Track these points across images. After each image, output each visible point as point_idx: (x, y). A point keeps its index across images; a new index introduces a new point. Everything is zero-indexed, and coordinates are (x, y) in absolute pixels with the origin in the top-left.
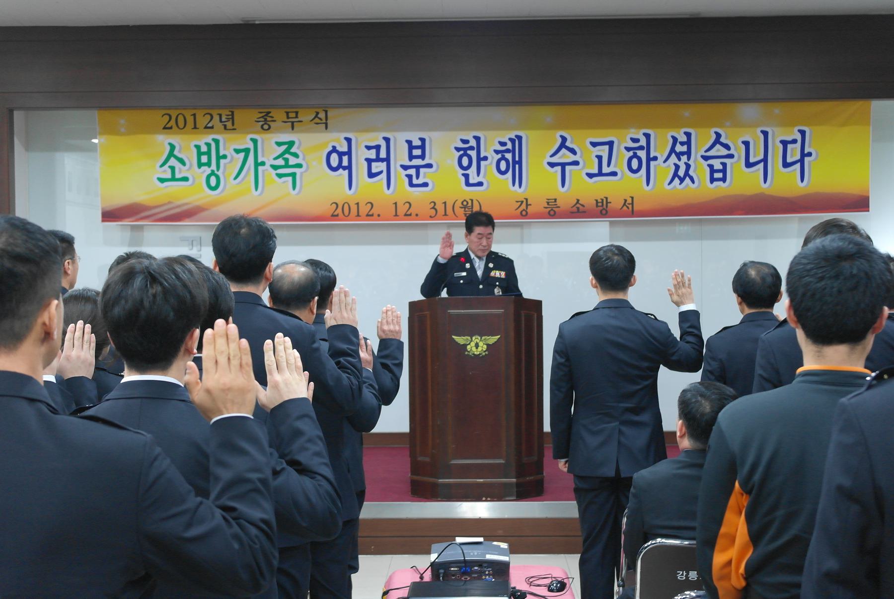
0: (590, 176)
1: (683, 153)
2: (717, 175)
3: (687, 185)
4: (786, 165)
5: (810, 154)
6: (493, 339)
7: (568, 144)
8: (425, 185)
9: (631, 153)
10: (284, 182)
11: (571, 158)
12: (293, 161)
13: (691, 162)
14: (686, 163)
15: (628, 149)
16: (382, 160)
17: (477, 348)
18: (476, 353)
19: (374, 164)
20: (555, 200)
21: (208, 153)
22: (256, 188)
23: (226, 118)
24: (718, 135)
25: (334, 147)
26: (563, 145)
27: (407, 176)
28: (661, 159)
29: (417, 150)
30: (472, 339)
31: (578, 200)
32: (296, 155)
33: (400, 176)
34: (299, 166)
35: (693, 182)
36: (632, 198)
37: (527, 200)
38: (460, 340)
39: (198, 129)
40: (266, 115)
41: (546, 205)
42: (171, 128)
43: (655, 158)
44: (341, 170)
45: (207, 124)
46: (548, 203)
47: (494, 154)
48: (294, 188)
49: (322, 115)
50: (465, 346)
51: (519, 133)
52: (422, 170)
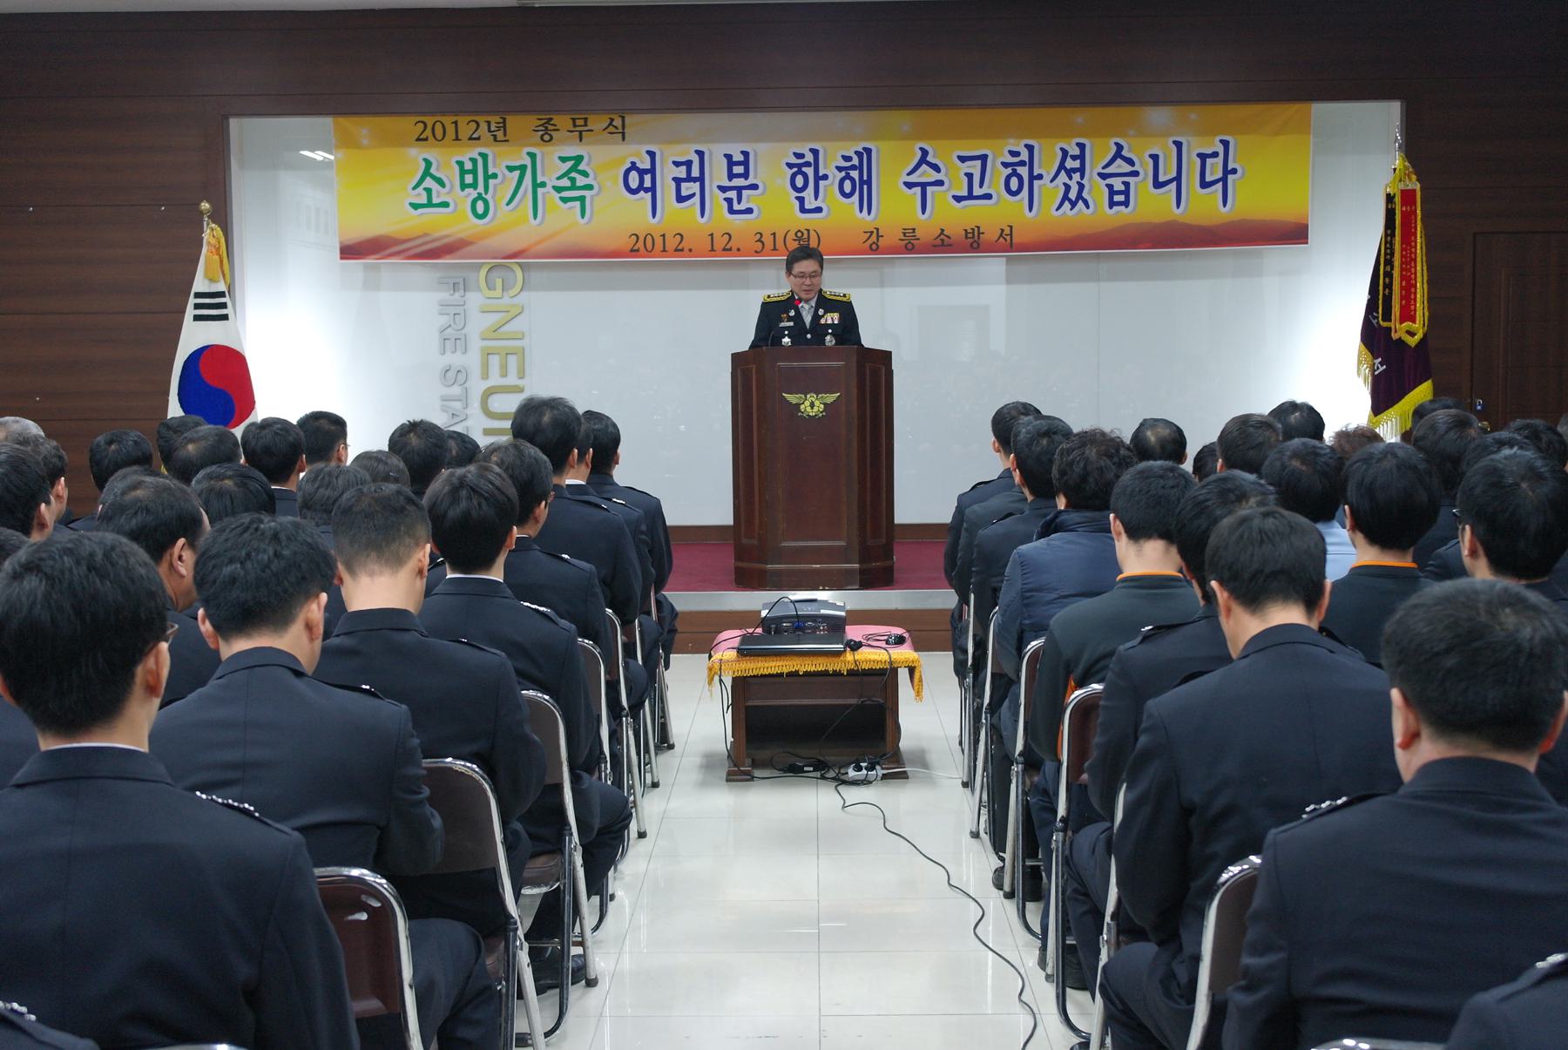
0: (958, 199)
1: (1074, 170)
2: (1118, 198)
3: (1080, 210)
4: (1205, 184)
5: (1234, 171)
6: (831, 398)
8: (749, 211)
9: (1009, 170)
10: (571, 208)
11: (932, 176)
12: (581, 181)
14: (1078, 183)
15: (1005, 165)
16: (694, 180)
17: (812, 408)
18: (811, 414)
19: (684, 185)
20: (914, 229)
21: (474, 172)
22: (535, 217)
24: (1120, 147)
25: (633, 164)
26: (923, 160)
27: (725, 199)
28: (1047, 178)
29: (739, 166)
30: (806, 397)
31: (943, 230)
32: (585, 174)
33: (716, 200)
34: (590, 187)
35: (1088, 207)
36: (1011, 227)
37: (877, 229)
38: (792, 398)
42: (426, 139)
43: (1040, 177)
46: (904, 234)
48: (583, 215)
49: (618, 122)
50: (798, 405)
51: (867, 145)
52: (745, 193)
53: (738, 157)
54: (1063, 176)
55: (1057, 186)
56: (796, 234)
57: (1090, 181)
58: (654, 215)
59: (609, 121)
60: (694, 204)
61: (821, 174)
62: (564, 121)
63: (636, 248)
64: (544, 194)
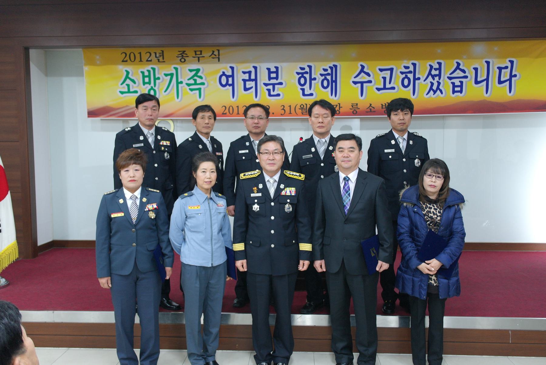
0: (379, 89)
1: (436, 75)
2: (456, 89)
3: (438, 95)
4: (500, 82)
5: (515, 76)
7: (365, 70)
8: (278, 95)
9: (404, 76)
10: (194, 94)
11: (367, 78)
12: (199, 81)
14: (438, 82)
15: (402, 73)
16: (252, 80)
19: (247, 83)
21: (149, 76)
22: (178, 98)
23: (159, 55)
24: (458, 64)
25: (224, 72)
26: (362, 71)
27: (267, 89)
28: (422, 79)
31: (371, 105)
32: (201, 77)
33: (263, 90)
34: (203, 84)
35: (442, 93)
37: (339, 104)
39: (142, 61)
40: (183, 53)
41: (352, 108)
42: (126, 61)
43: (419, 79)
44: (228, 86)
46: (352, 106)
48: (200, 97)
49: (216, 53)
52: (276, 86)
54: (430, 78)
55: (427, 83)
57: (443, 80)
59: (212, 52)
60: (252, 92)
61: (312, 78)
62: (190, 52)
63: (225, 112)
64: (182, 87)
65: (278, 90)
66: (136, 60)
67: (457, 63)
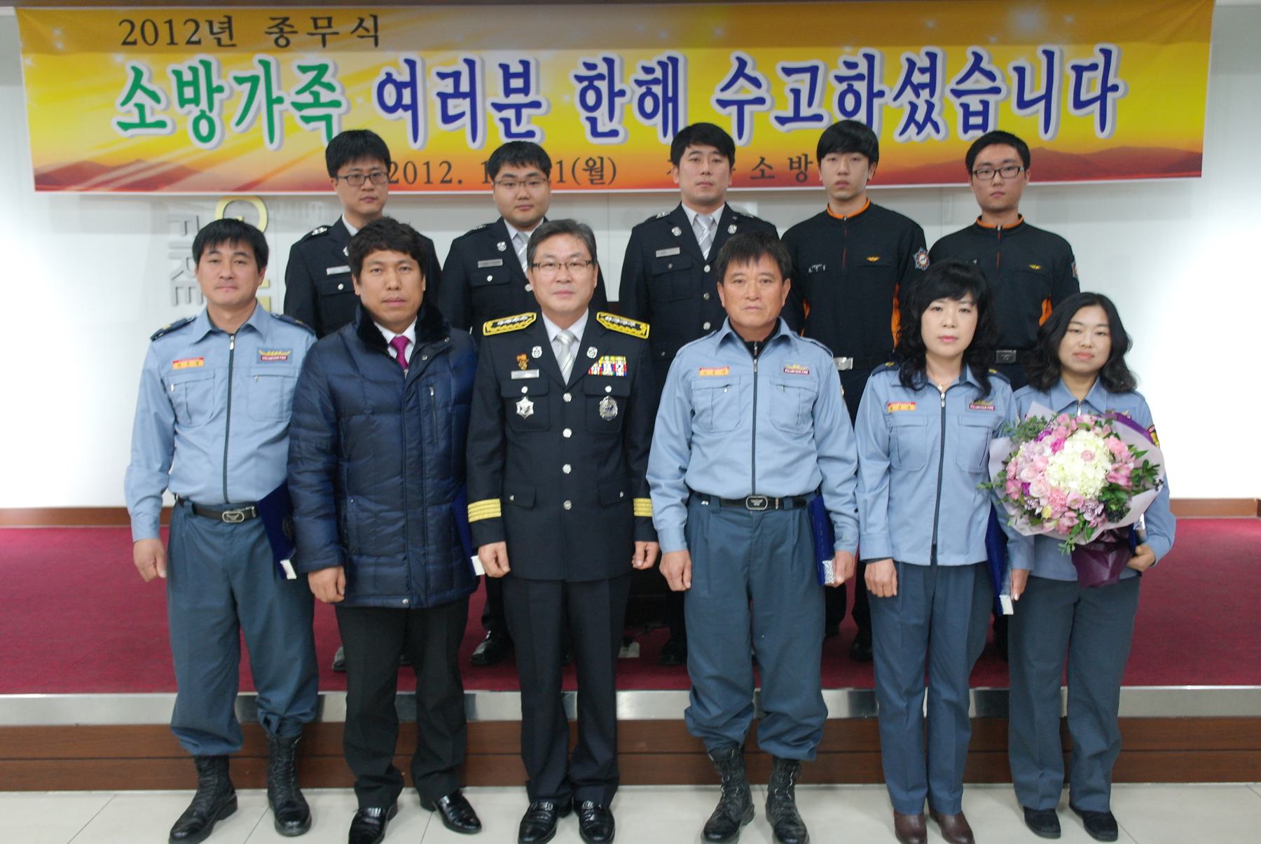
0: (782, 120)
1: (923, 86)
3: (929, 135)
4: (1079, 104)
5: (1115, 88)
9: (844, 86)
10: (314, 130)
11: (751, 92)
12: (326, 96)
13: (935, 100)
14: (927, 102)
15: (840, 79)
16: (464, 96)
19: (451, 102)
21: (195, 83)
22: (272, 140)
23: (221, 28)
25: (389, 75)
26: (740, 73)
27: (502, 120)
28: (889, 95)
31: (763, 159)
32: (330, 87)
34: (336, 104)
35: (937, 130)
39: (177, 44)
42: (135, 43)
43: (881, 94)
45: (191, 37)
47: (635, 87)
49: (369, 23)
51: (674, 53)
52: (525, 112)
53: (516, 68)
54: (909, 94)
55: (901, 106)
56: (587, 163)
58: (415, 138)
62: (300, 17)
64: (281, 113)
65: (529, 122)
66: (158, 42)
67: (975, 54)
